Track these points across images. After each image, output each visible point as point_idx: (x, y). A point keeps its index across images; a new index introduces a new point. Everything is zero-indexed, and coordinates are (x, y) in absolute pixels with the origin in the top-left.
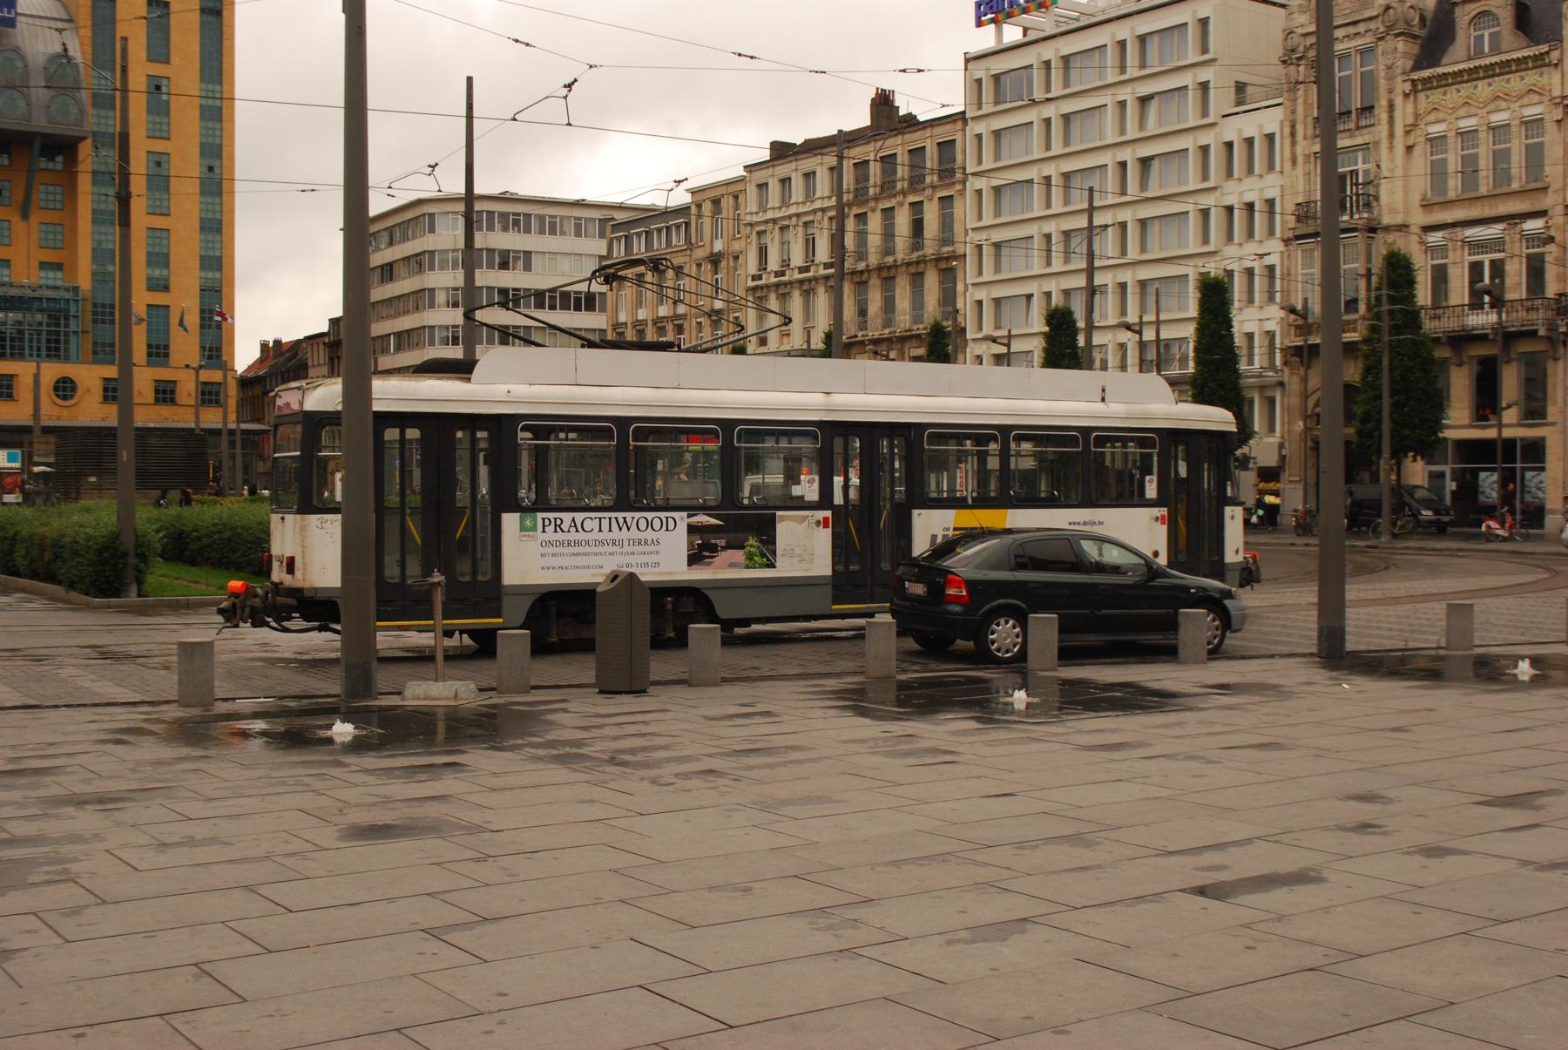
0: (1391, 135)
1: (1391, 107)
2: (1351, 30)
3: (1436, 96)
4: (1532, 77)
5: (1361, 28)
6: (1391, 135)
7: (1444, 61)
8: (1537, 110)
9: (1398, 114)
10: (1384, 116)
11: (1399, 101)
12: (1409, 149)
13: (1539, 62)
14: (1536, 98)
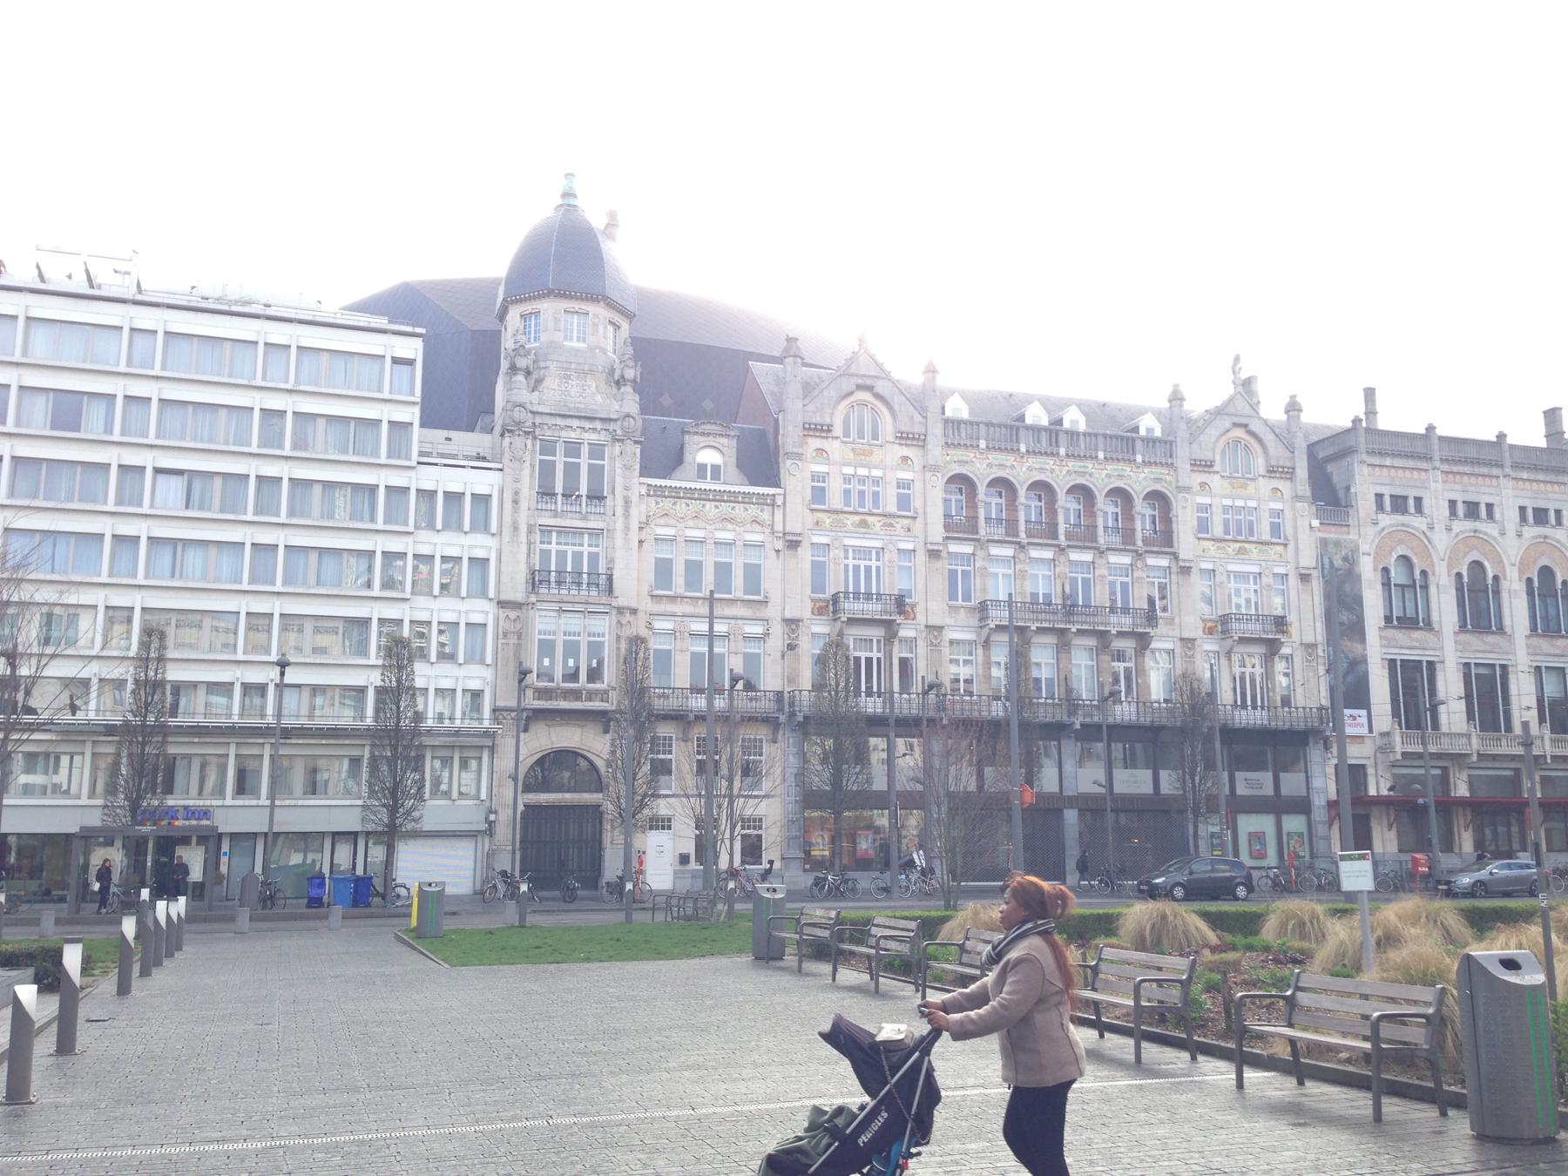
0: (627, 528)
1: (627, 502)
2: (587, 425)
3: (666, 504)
4: (754, 510)
5: (598, 425)
6: (627, 528)
7: (677, 473)
8: (757, 538)
9: (634, 511)
10: (619, 511)
11: (635, 499)
12: (641, 542)
13: (762, 500)
14: (758, 528)
